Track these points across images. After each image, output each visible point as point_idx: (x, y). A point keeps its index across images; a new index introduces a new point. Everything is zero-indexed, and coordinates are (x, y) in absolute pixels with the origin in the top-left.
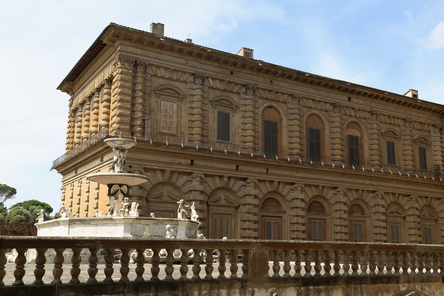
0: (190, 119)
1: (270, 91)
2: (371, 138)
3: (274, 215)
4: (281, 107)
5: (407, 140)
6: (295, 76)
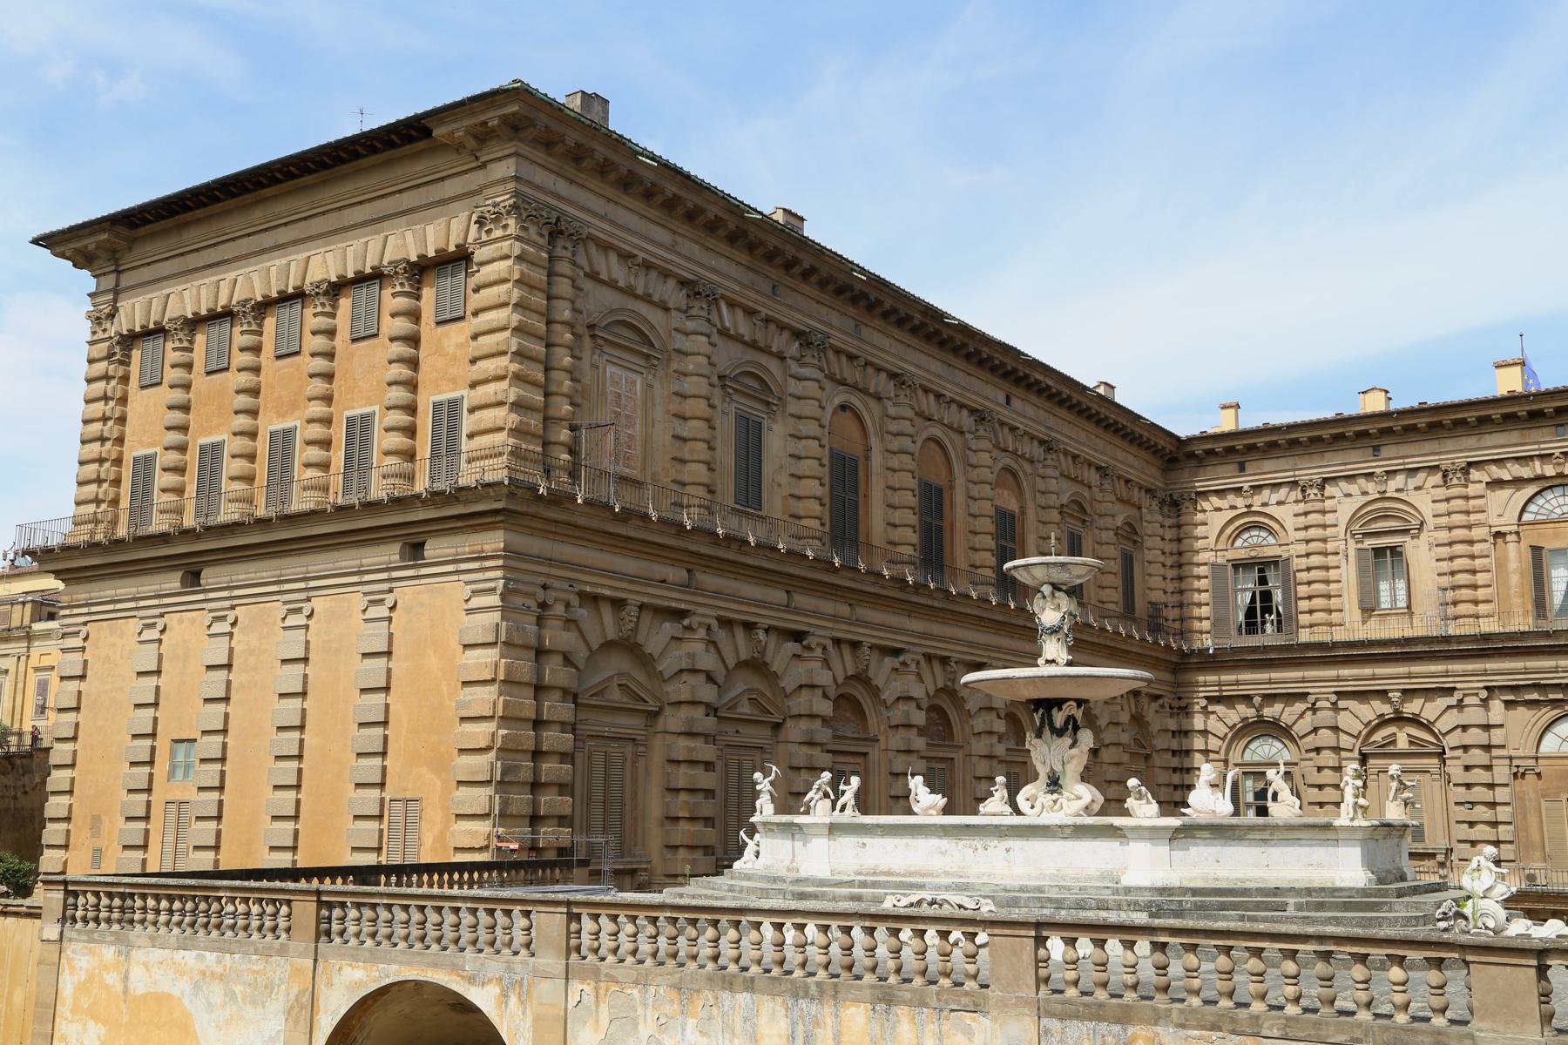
0: (679, 432)
1: (851, 357)
2: (1044, 519)
3: (852, 749)
4: (868, 409)
5: (1107, 529)
6: (918, 318)
